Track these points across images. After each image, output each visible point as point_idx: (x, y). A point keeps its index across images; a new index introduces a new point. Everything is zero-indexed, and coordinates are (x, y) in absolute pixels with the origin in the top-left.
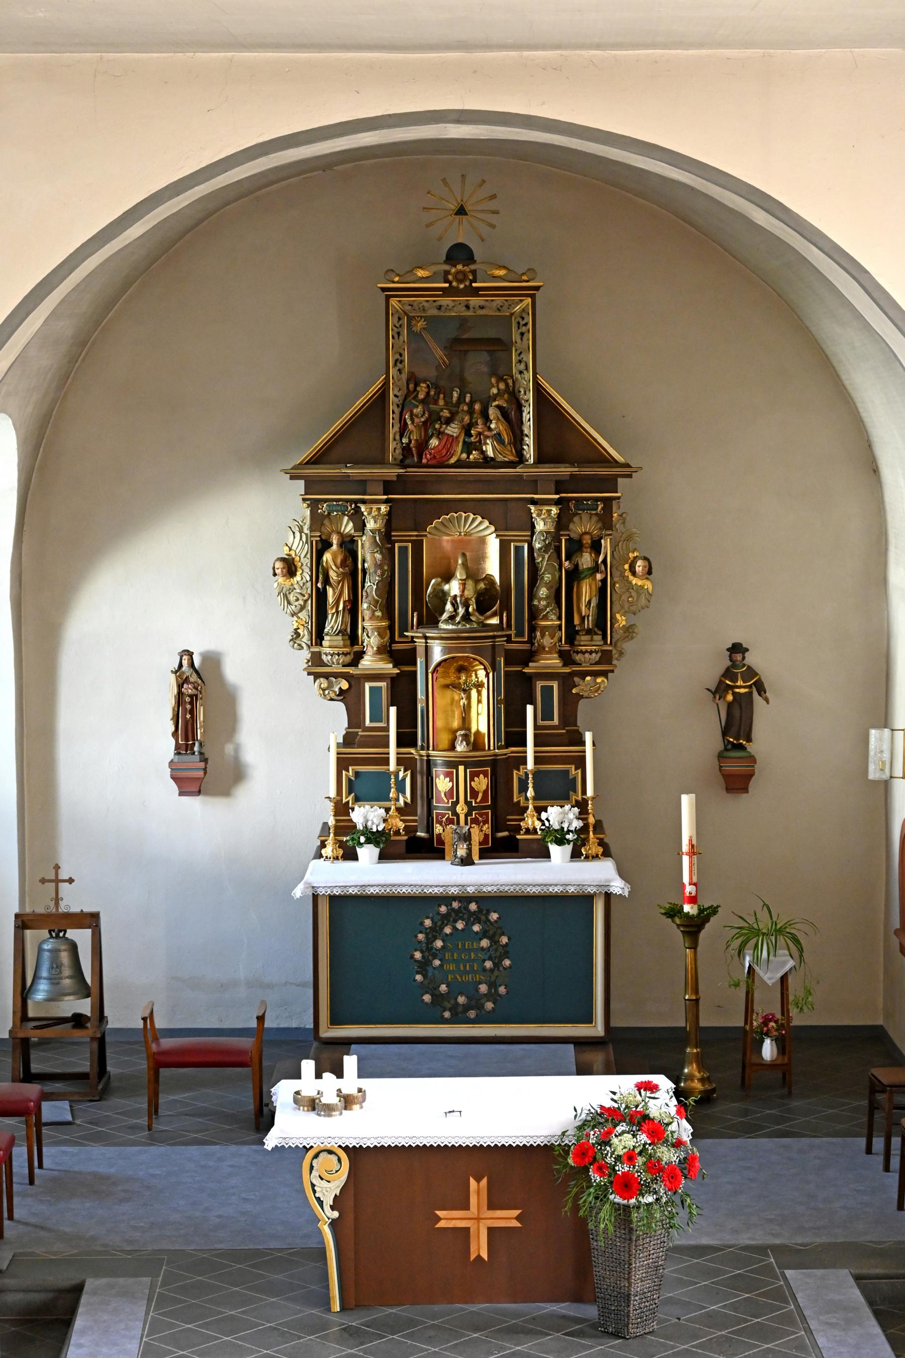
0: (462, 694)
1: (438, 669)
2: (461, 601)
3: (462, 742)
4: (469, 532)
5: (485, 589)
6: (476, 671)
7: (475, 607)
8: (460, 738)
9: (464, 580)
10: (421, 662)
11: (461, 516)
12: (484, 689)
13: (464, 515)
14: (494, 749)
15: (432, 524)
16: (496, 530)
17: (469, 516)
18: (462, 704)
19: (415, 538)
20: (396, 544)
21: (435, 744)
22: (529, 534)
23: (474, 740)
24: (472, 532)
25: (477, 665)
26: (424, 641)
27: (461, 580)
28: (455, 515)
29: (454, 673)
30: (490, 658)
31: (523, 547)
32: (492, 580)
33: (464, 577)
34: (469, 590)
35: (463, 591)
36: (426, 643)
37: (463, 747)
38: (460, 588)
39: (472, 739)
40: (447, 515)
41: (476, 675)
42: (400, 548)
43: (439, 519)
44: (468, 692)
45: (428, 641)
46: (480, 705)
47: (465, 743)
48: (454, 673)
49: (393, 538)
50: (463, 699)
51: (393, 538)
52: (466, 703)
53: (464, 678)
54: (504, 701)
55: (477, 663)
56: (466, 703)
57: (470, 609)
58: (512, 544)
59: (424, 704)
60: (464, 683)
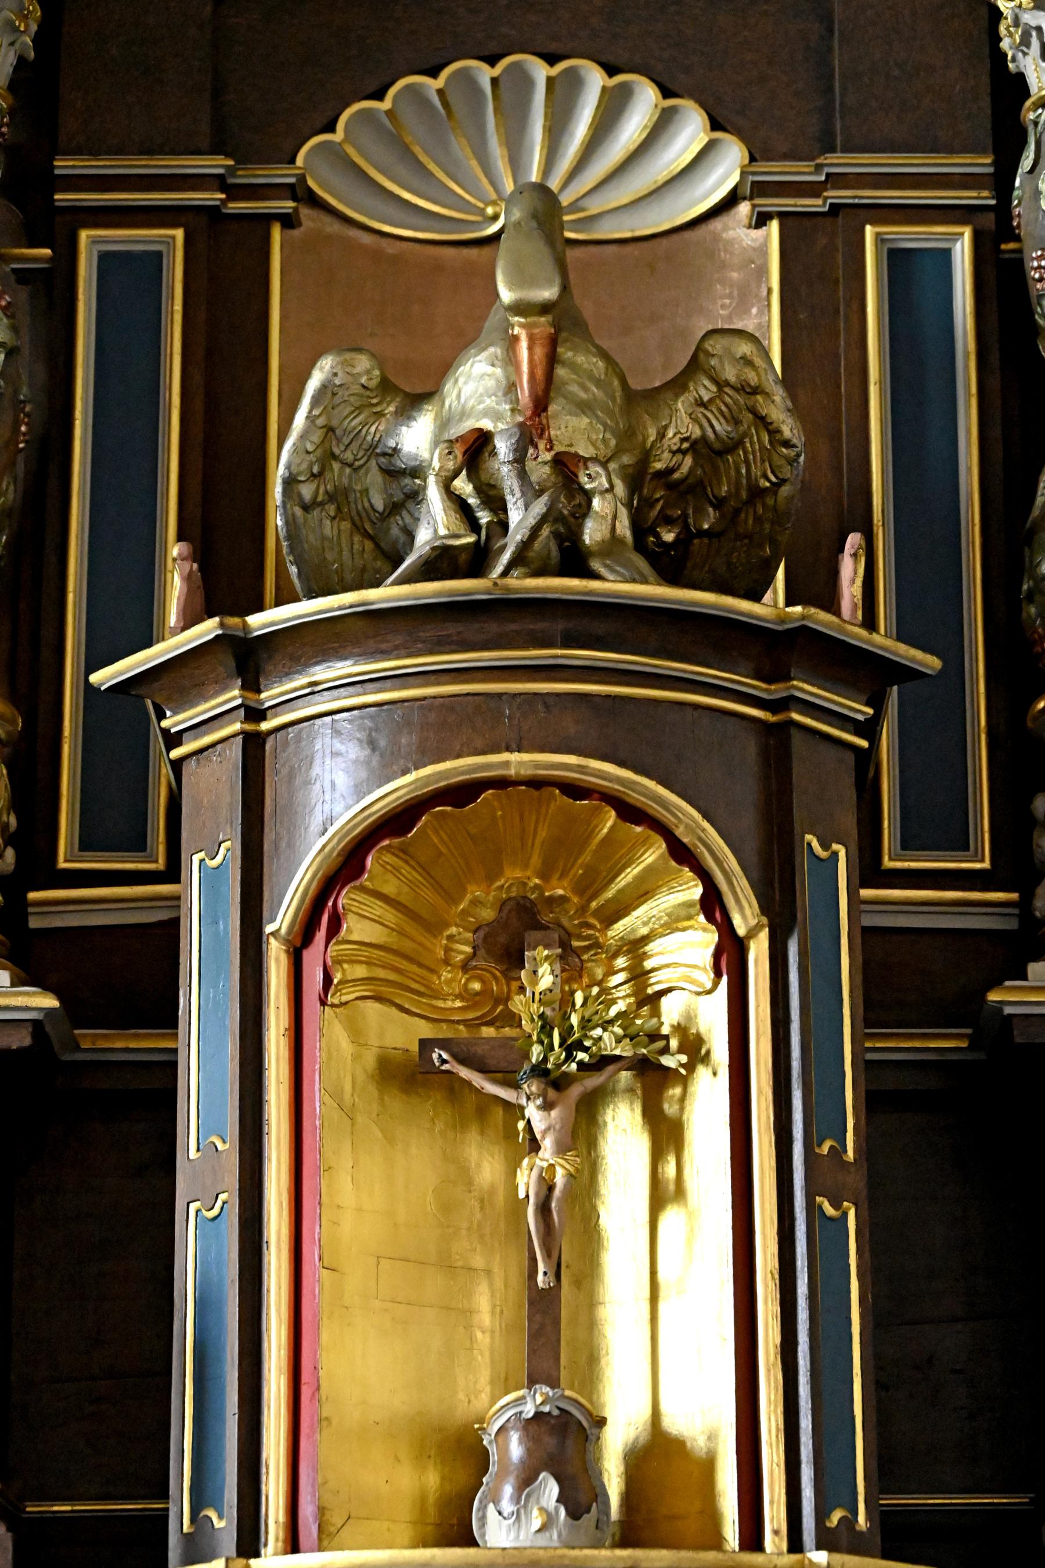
0: (532, 1111)
1: (346, 898)
2: (519, 460)
3: (527, 1480)
4: (574, 207)
5: (696, 447)
6: (636, 947)
7: (624, 528)
8: (516, 1449)
9: (545, 308)
10: (212, 878)
11: (524, 81)
12: (702, 1072)
13: (541, 72)
14: (795, 1545)
15: (331, 128)
16: (753, 159)
17: (573, 82)
18: (526, 1181)
19: (214, 197)
20: (84, 235)
21: (307, 1510)
22: (983, 163)
23: (628, 1498)
24: (595, 206)
25: (642, 893)
26: (233, 696)
27: (519, 308)
28: (484, 73)
29: (465, 967)
30: (749, 821)
31: (945, 256)
32: (747, 361)
33: (548, 293)
34: (584, 407)
35: (540, 405)
36: (255, 714)
37: (537, 1522)
38: (511, 388)
39: (614, 1485)
40: (433, 72)
41: (639, 976)
42: (108, 262)
43: (379, 95)
44: (575, 1091)
45: (270, 696)
46: (671, 1217)
47: (550, 1489)
48: (465, 967)
49: (61, 197)
50: (534, 1146)
51: (61, 197)
52: (560, 1178)
53: (546, 980)
54: (857, 1181)
55: (654, 853)
56: (560, 1178)
57: (592, 533)
58: (869, 230)
59: (229, 1197)
60: (546, 1028)
